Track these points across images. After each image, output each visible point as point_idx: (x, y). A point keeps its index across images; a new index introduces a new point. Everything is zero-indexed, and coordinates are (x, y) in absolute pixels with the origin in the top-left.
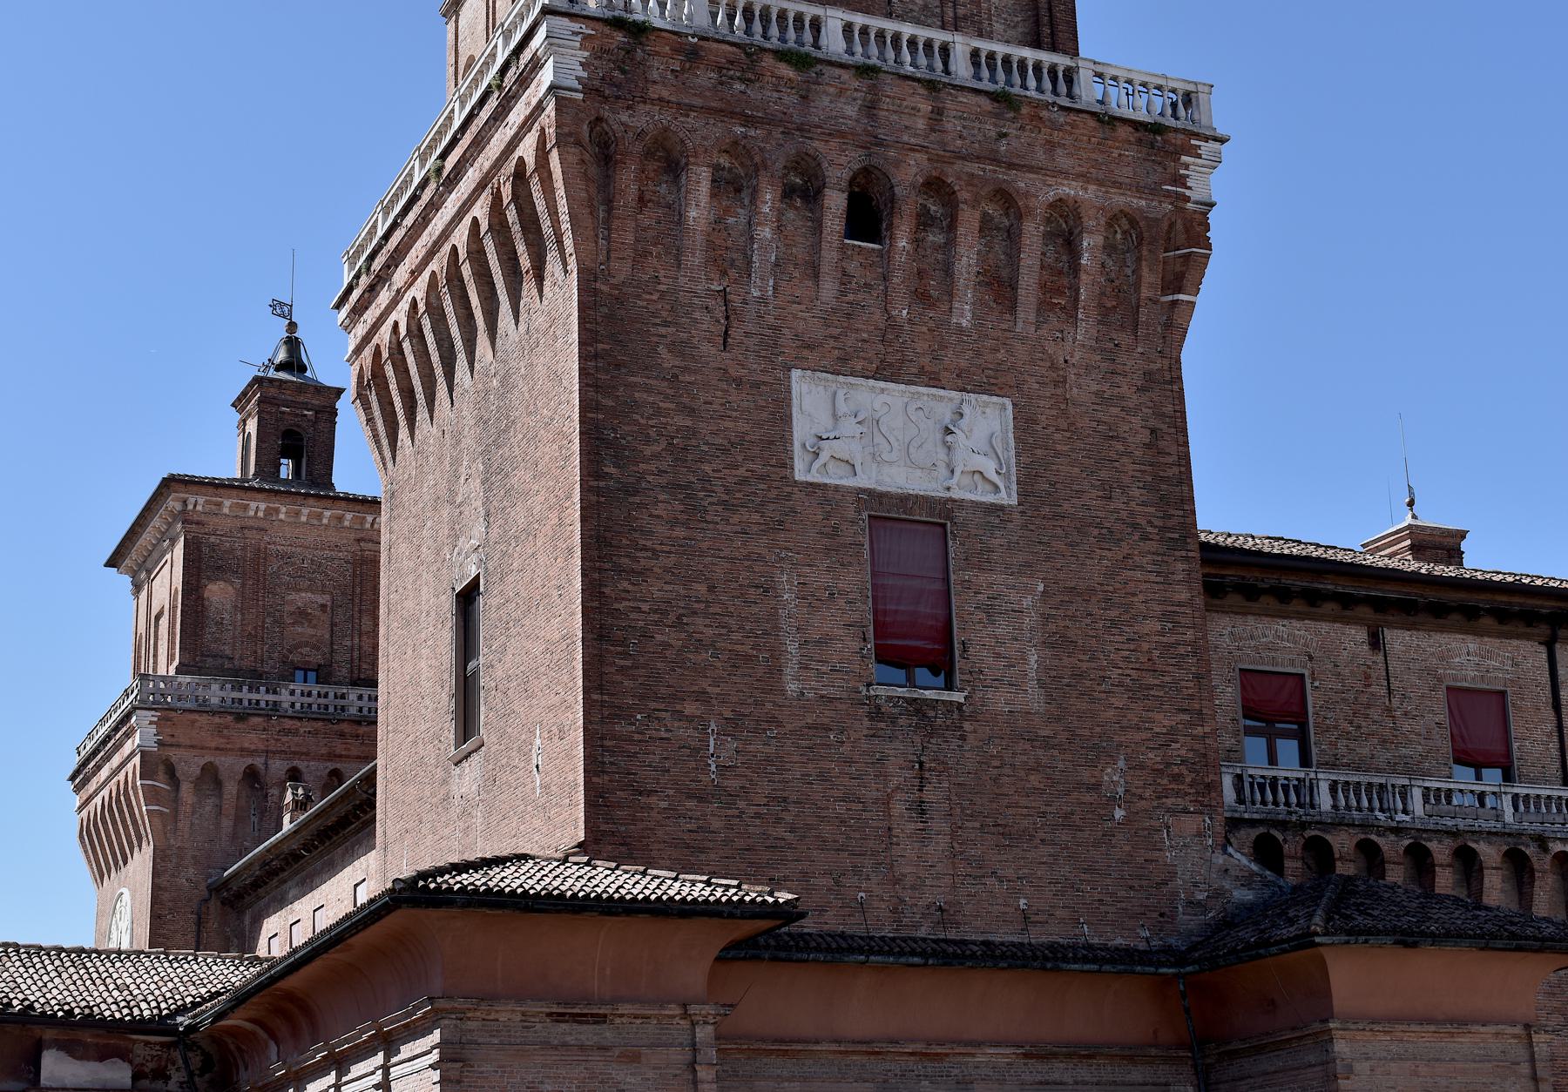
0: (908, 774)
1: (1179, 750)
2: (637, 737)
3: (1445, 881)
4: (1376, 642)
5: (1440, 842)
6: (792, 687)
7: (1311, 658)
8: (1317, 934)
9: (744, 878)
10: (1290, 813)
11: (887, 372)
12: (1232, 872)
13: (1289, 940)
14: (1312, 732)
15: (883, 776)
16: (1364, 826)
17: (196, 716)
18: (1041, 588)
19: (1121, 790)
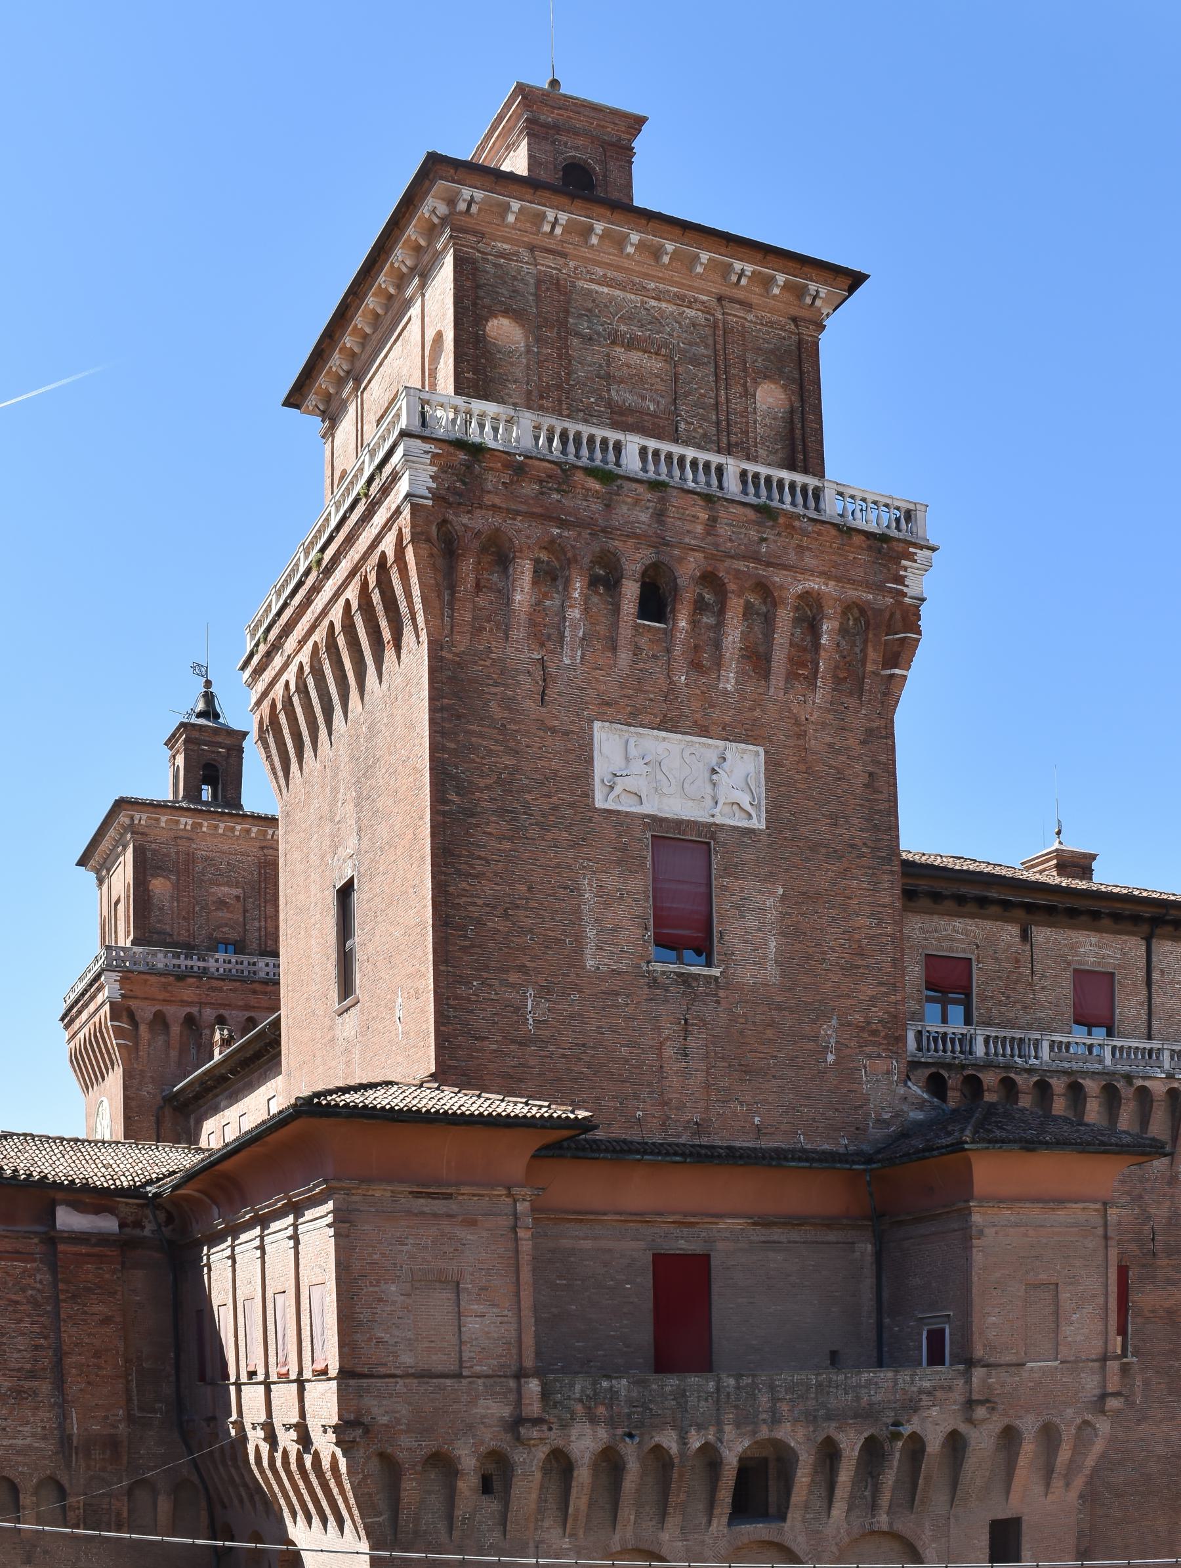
0: (676, 1027)
1: (877, 1013)
2: (473, 998)
3: (1059, 1106)
4: (1025, 936)
5: (1058, 1079)
6: (590, 963)
7: (978, 947)
8: (967, 1143)
9: (553, 1100)
10: (954, 1058)
11: (667, 724)
12: (910, 1100)
13: (947, 1146)
14: (975, 1000)
15: (657, 1029)
16: (1007, 1067)
17: (147, 977)
18: (781, 891)
19: (833, 1041)
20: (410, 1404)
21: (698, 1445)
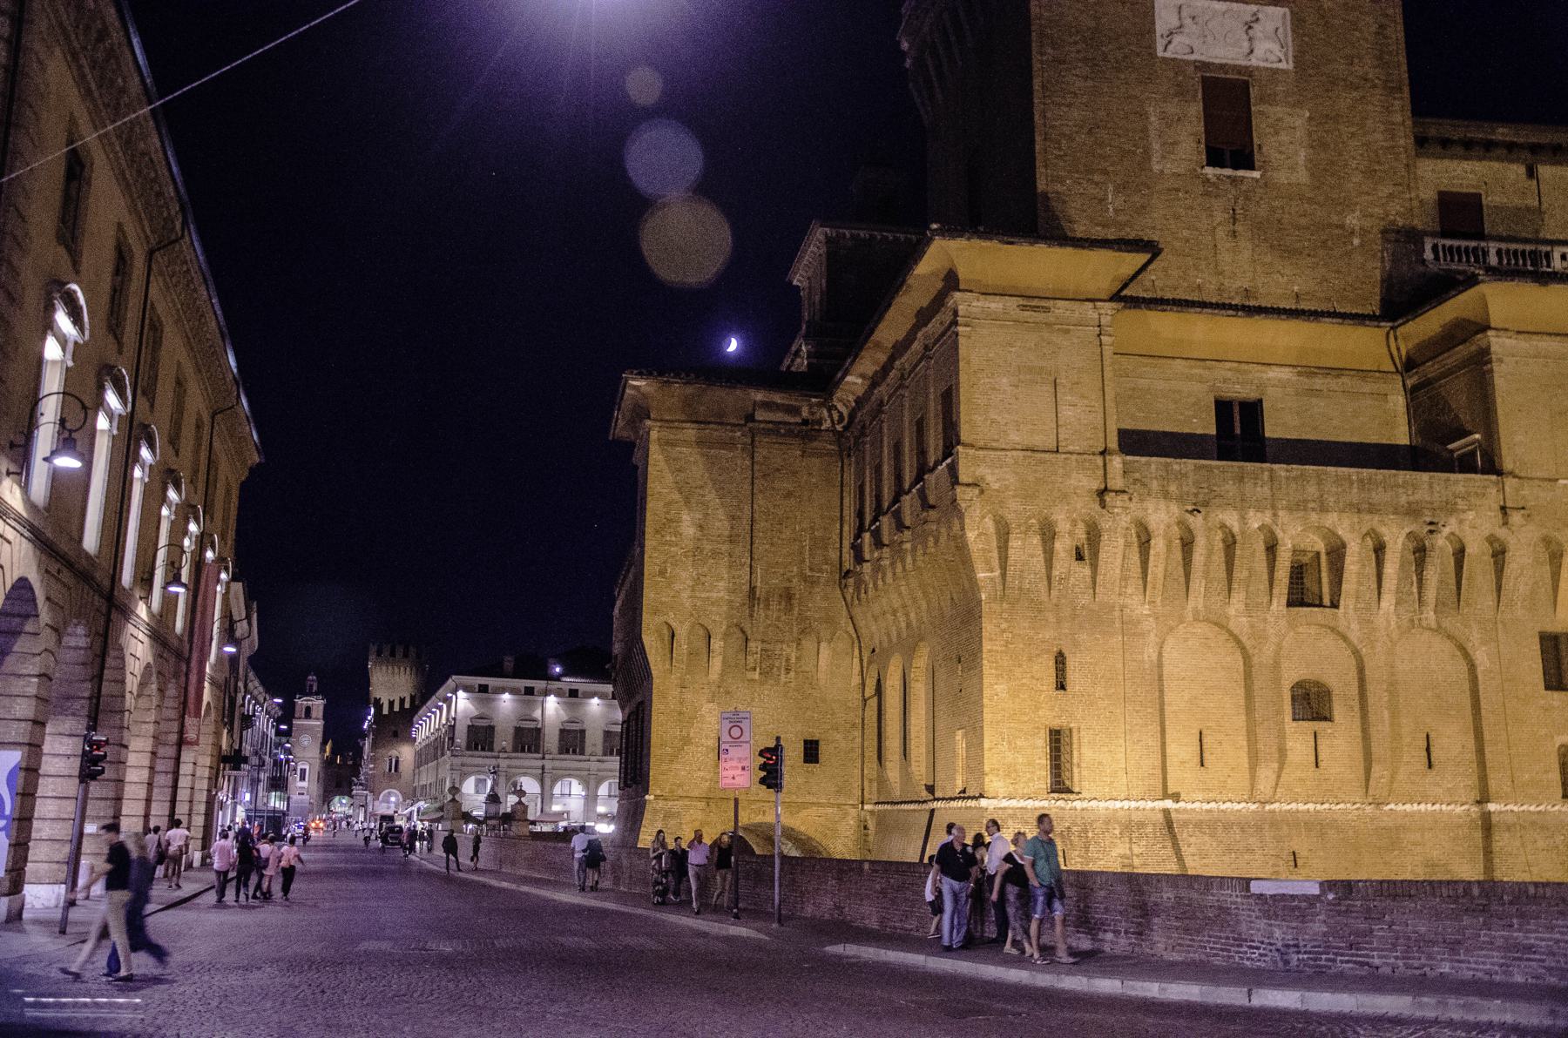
0: (1226, 216)
4: (1531, 173)
6: (1156, 168)
18: (1308, 114)
20: (1017, 473)
21: (1256, 526)
